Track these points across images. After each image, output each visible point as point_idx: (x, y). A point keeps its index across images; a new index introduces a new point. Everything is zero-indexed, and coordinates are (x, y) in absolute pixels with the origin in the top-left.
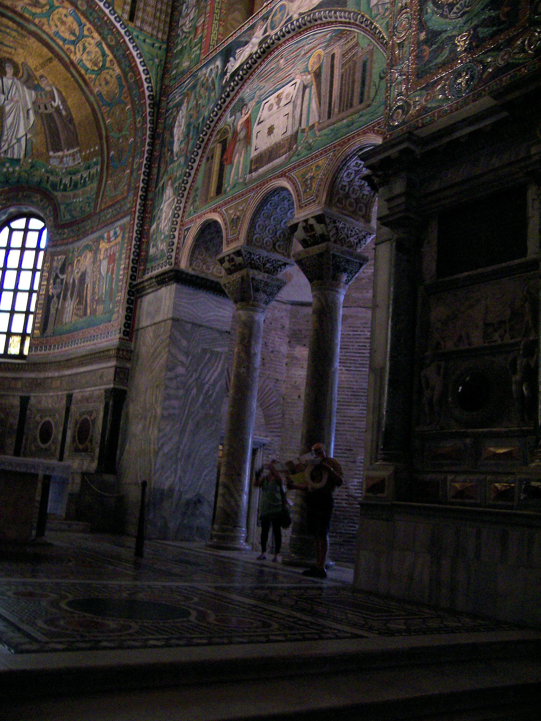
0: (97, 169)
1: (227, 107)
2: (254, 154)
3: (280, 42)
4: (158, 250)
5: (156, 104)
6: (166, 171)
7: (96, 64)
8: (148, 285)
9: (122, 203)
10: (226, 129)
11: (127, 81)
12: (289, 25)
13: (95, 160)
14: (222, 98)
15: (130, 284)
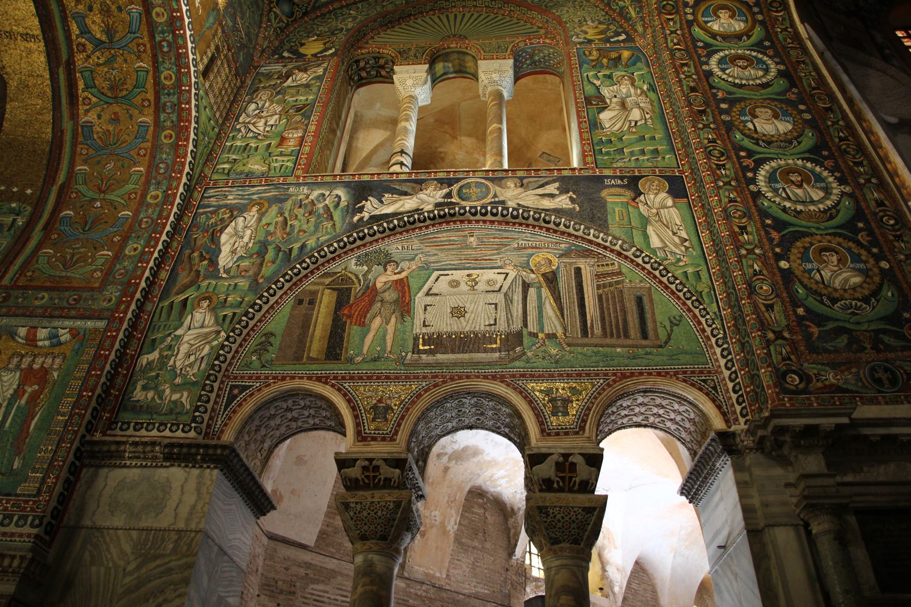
0: (14, 220)
1: (352, 250)
2: (418, 329)
3: (472, 218)
4: (160, 398)
5: (189, 189)
6: (194, 282)
7: (112, 88)
8: (130, 452)
9: (84, 295)
10: (350, 278)
11: (156, 137)
12: (500, 209)
13: (14, 205)
14: (352, 235)
15: (83, 436)
